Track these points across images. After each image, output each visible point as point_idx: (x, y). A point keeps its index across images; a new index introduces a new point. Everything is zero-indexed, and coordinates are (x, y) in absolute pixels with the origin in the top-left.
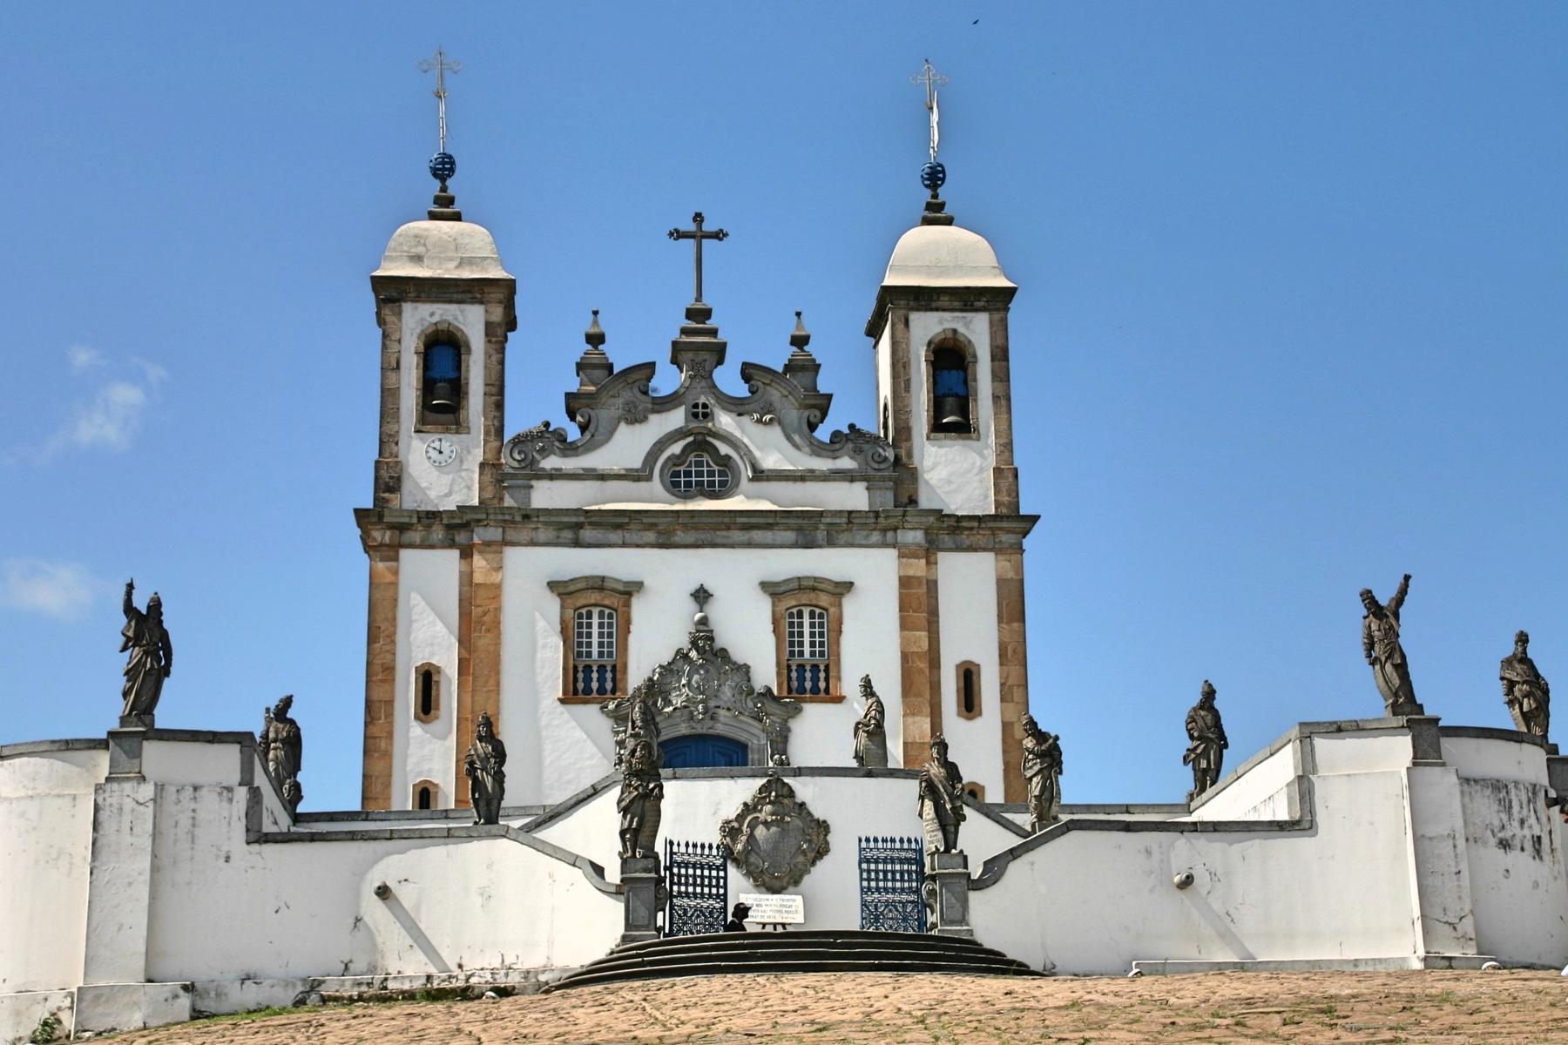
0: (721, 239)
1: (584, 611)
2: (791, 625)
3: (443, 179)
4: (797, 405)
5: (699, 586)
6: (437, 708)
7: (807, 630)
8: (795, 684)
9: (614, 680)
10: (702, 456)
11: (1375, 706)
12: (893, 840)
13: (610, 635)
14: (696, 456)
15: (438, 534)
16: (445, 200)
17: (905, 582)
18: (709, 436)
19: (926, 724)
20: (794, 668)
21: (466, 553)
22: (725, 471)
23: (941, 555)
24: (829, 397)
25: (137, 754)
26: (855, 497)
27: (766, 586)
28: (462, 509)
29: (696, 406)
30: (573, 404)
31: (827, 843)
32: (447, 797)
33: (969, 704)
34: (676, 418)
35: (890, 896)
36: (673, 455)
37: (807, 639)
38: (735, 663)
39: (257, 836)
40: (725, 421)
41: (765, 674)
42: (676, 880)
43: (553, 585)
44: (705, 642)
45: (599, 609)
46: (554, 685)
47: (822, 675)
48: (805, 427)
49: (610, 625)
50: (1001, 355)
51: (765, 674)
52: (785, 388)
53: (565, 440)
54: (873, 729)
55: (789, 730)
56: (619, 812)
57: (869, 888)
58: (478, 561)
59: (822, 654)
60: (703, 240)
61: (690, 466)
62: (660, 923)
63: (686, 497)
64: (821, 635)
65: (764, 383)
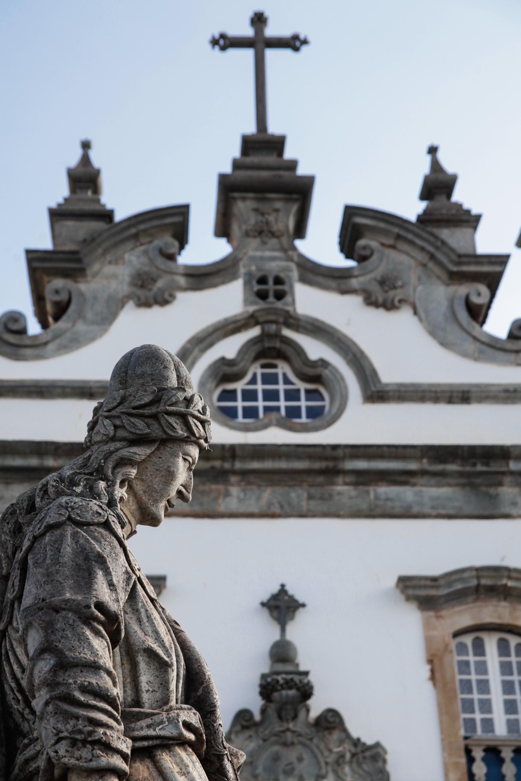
0: (296, 49)
4: (444, 276)
5: (275, 589)
10: (275, 366)
14: (263, 366)
18: (289, 326)
20: (478, 754)
22: (317, 391)
29: (262, 281)
36: (223, 361)
38: (357, 742)
48: (463, 315)
52: (422, 249)
53: (23, 331)
61: (253, 381)
63: (246, 429)
65: (383, 245)
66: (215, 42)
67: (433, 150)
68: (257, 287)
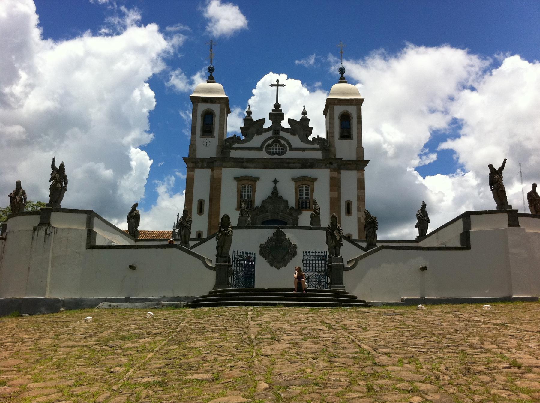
1: (244, 186)
2: (300, 190)
3: (211, 73)
6: (204, 212)
7: (304, 191)
8: (301, 206)
9: (251, 204)
11: (493, 205)
12: (316, 252)
13: (251, 192)
17: (332, 179)
21: (212, 170)
23: (342, 171)
24: (312, 128)
25: (49, 217)
26: (318, 155)
27: (293, 179)
29: (276, 131)
31: (296, 252)
33: (349, 212)
34: (270, 134)
35: (314, 273)
36: (268, 144)
37: (304, 194)
39: (91, 246)
40: (283, 134)
42: (238, 266)
43: (235, 178)
44: (275, 194)
45: (248, 185)
47: (308, 204)
49: (251, 190)
51: (292, 202)
55: (298, 218)
56: (216, 240)
57: (306, 270)
58: (216, 172)
59: (308, 198)
60: (279, 87)
62: (230, 281)
64: (308, 193)
66: (270, 85)
67: (304, 106)
68: (275, 132)
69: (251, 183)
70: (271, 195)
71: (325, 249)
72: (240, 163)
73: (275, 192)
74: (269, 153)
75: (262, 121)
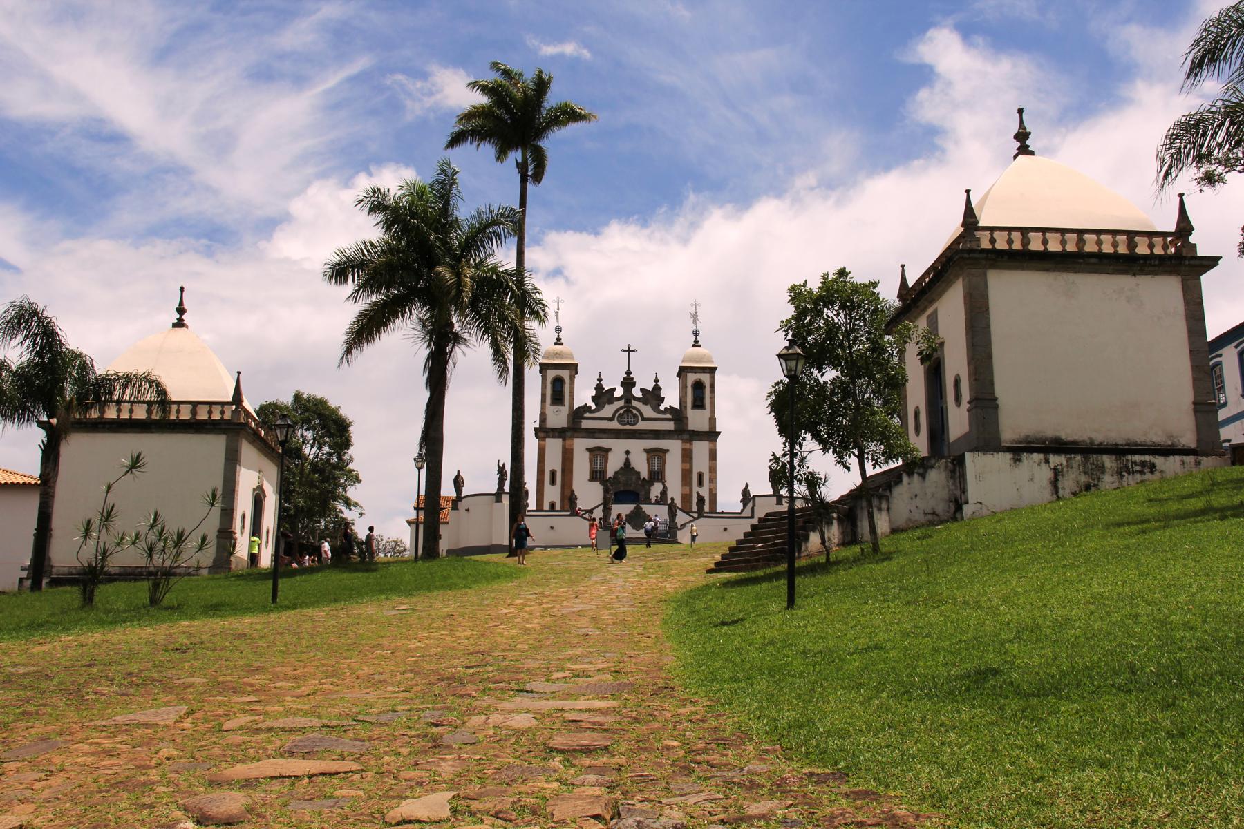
11: (771, 492)
15: (557, 434)
16: (559, 339)
17: (683, 450)
19: (688, 488)
21: (564, 440)
24: (664, 398)
26: (670, 426)
28: (563, 428)
30: (593, 399)
32: (558, 507)
33: (700, 483)
34: (622, 403)
40: (634, 403)
41: (644, 474)
43: (588, 449)
46: (588, 477)
50: (712, 386)
51: (644, 474)
54: (664, 493)
58: (568, 442)
69: (604, 454)
70: (622, 466)
71: (667, 517)
72: (592, 433)
73: (627, 463)
74: (620, 422)
75: (614, 389)
